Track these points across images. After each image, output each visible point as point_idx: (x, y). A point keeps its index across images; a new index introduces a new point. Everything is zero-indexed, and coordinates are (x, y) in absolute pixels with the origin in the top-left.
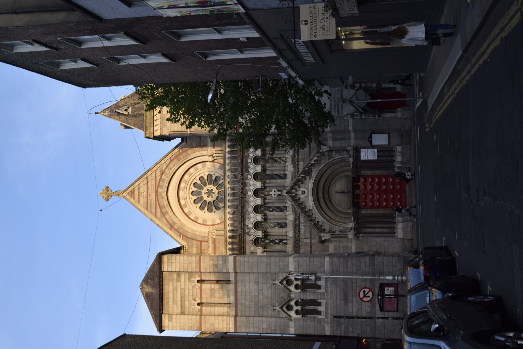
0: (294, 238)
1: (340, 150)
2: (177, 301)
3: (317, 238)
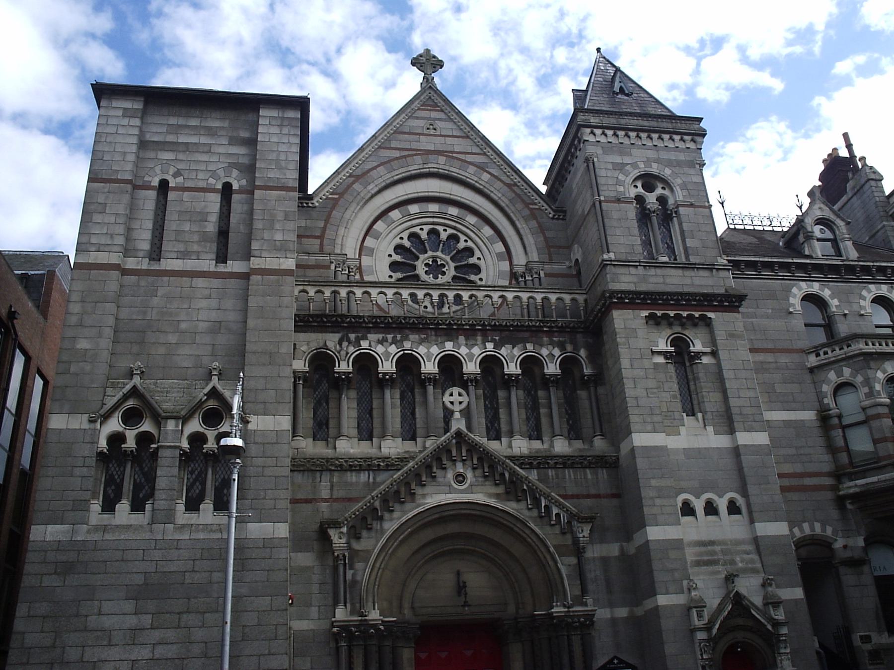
2: (177, 134)
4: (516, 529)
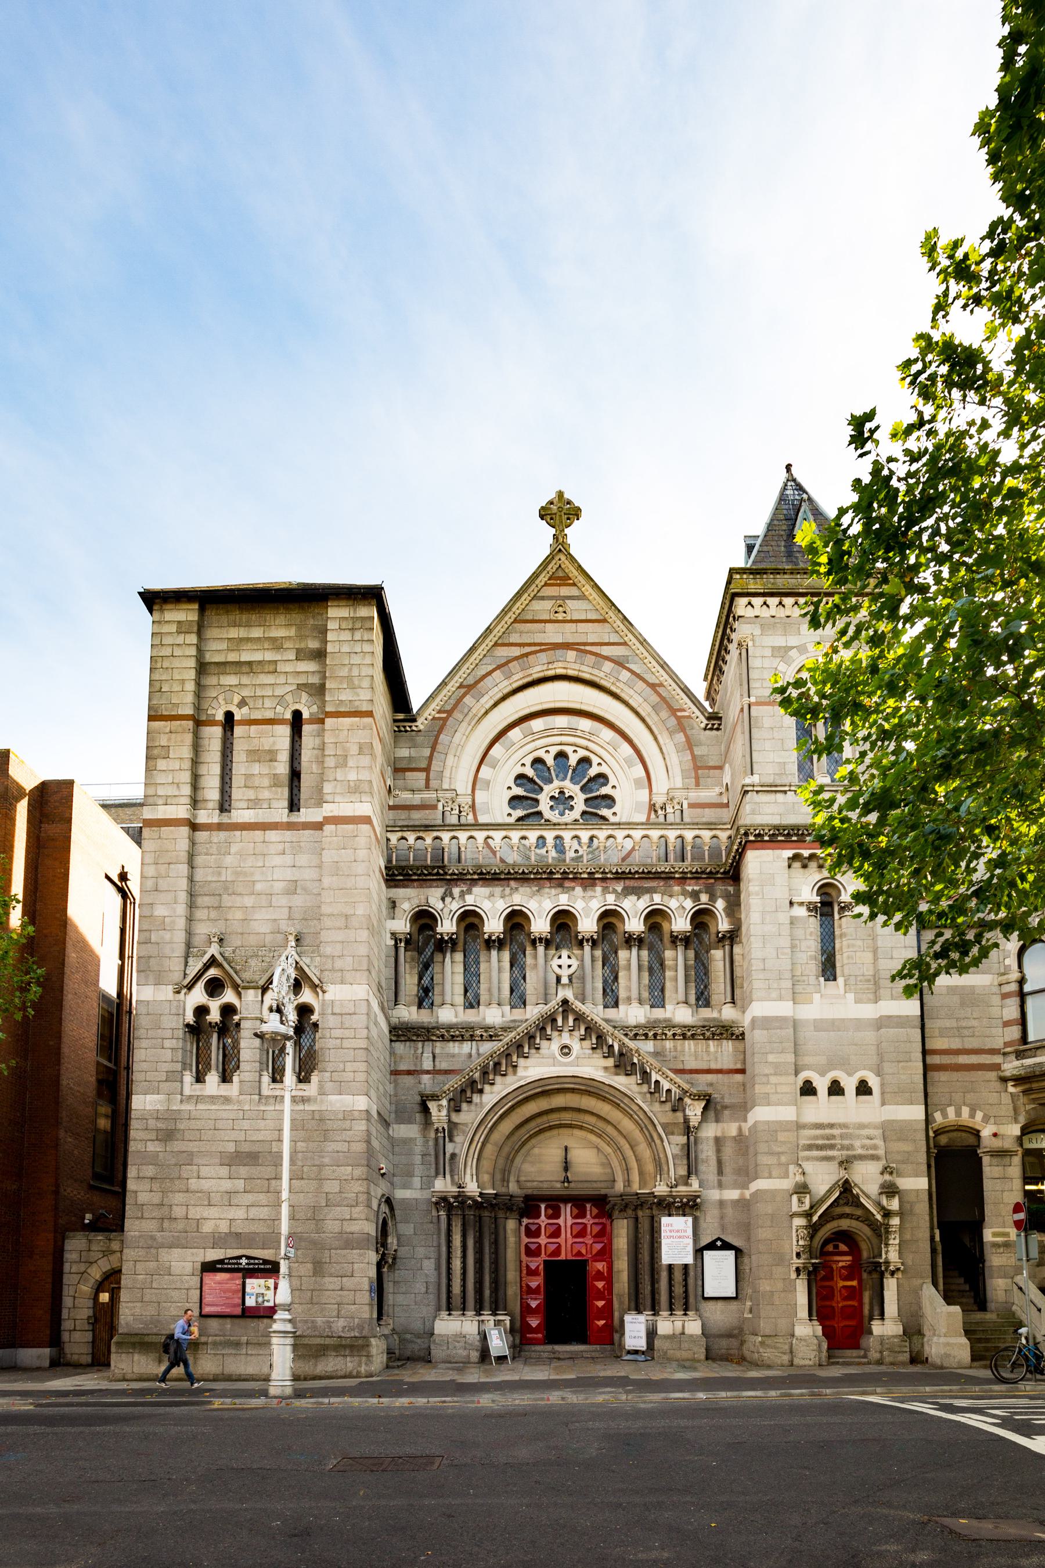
1: (689, 1156)
3: (437, 1090)
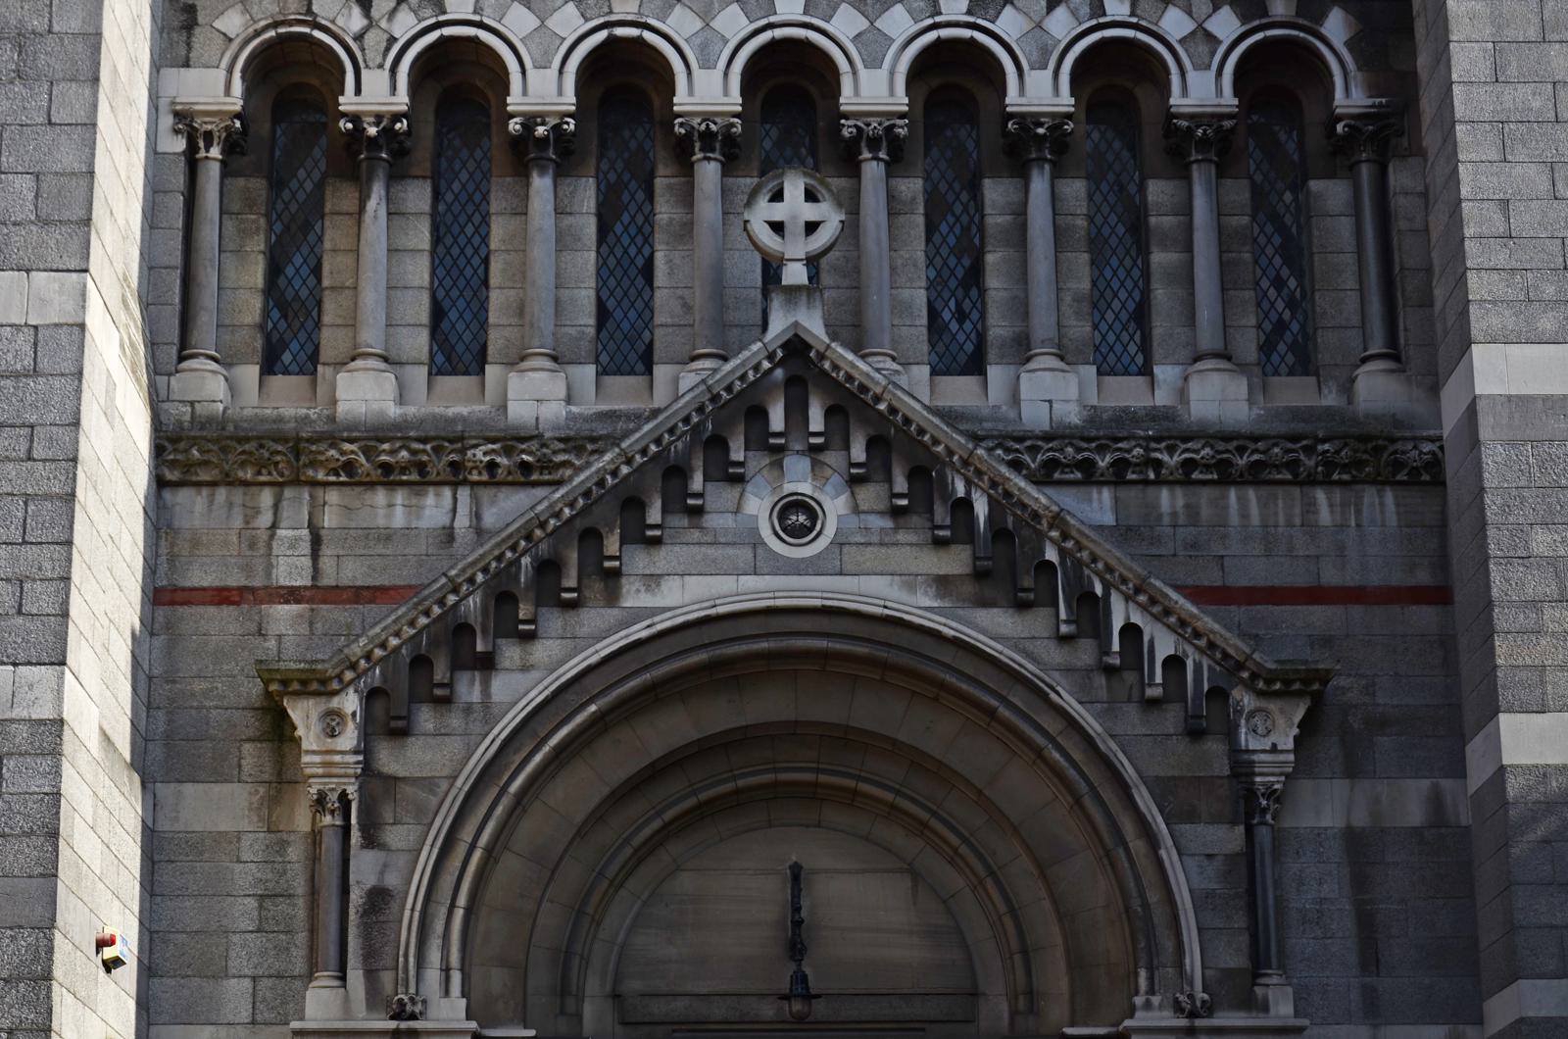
0: (320, 427)
3: (323, 655)
4: (1004, 712)
